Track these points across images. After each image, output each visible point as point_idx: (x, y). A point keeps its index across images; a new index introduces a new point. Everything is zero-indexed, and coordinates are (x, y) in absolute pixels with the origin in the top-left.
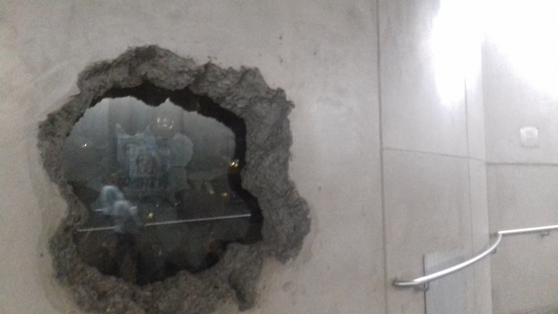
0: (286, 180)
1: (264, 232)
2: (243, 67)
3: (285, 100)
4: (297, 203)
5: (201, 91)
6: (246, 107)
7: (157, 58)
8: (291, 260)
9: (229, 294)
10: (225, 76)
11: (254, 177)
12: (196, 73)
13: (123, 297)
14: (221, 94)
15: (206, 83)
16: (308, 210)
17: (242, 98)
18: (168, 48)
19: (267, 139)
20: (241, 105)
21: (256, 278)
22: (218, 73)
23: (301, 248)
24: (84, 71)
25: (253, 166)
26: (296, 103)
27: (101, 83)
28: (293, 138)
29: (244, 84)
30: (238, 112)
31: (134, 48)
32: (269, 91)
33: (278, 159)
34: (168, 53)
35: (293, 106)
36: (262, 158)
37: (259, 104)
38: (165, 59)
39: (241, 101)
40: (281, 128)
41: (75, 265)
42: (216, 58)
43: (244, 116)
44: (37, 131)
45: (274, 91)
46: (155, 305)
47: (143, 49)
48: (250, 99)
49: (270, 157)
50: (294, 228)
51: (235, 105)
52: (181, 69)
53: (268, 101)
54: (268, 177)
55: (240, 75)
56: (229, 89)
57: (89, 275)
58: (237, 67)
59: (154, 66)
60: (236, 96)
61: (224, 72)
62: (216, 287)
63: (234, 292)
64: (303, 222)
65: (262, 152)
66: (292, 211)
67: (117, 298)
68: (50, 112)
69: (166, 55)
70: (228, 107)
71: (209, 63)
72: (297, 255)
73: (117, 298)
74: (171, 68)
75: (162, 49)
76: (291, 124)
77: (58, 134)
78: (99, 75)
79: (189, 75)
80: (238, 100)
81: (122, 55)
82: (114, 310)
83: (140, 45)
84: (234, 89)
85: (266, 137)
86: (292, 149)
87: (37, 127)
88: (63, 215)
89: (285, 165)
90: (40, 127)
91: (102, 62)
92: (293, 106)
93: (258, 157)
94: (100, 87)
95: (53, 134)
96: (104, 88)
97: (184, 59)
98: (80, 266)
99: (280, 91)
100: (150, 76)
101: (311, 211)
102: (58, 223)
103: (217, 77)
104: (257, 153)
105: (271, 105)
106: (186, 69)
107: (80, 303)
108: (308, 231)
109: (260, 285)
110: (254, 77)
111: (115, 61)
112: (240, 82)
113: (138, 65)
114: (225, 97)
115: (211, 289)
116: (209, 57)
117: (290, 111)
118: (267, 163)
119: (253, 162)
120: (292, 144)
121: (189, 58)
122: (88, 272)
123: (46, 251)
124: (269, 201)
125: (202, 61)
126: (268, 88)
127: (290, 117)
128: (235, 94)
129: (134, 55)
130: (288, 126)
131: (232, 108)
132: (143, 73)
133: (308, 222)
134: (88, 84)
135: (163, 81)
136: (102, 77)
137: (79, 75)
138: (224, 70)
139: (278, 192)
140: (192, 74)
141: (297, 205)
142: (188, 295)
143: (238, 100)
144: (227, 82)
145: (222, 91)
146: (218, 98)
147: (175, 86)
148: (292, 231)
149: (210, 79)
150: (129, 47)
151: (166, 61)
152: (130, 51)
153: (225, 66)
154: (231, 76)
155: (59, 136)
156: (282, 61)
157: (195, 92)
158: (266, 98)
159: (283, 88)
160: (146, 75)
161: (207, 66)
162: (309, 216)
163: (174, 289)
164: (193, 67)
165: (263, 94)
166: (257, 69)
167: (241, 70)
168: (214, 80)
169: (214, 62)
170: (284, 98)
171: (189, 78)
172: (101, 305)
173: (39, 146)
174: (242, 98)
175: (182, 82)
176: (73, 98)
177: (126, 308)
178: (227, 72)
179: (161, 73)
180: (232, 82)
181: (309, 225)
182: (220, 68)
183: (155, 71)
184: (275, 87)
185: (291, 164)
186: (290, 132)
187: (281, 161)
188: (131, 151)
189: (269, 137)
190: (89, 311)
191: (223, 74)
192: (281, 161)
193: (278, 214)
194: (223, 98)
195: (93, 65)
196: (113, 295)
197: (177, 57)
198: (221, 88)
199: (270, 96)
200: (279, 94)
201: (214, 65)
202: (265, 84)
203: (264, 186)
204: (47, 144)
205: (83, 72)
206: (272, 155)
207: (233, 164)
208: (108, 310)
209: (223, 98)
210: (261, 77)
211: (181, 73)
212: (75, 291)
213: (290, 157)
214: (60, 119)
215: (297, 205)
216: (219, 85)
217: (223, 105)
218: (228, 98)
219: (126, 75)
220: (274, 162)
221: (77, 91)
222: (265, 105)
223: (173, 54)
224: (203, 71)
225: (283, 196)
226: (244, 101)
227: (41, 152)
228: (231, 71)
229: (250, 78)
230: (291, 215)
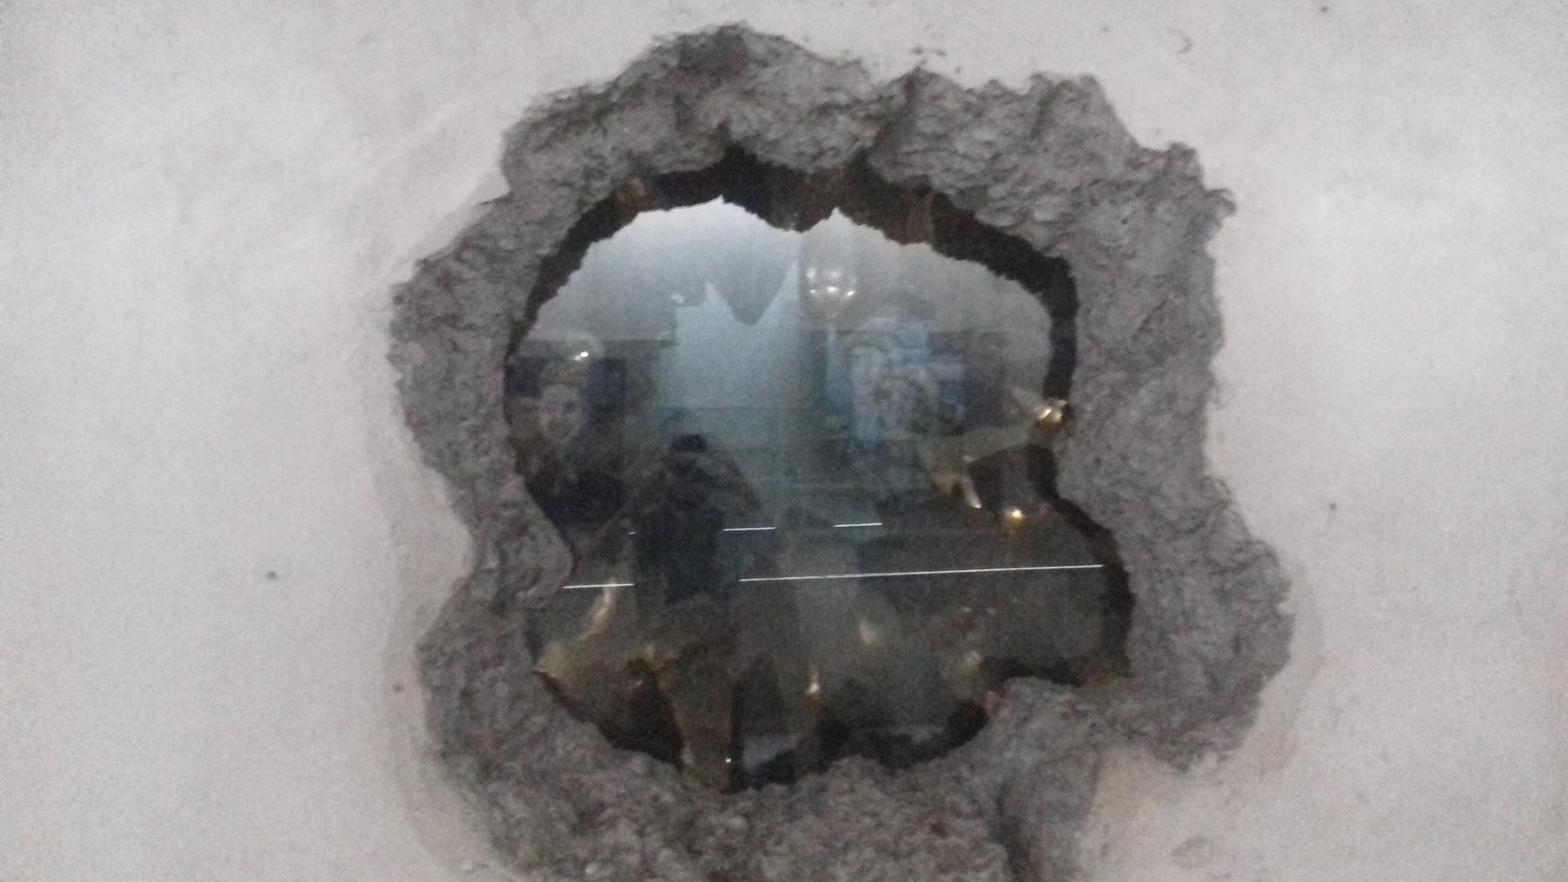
0: (1199, 479)
1: (1136, 651)
2: (1038, 77)
3: (1201, 187)
4: (1241, 558)
5: (908, 172)
6: (1066, 220)
7: (753, 67)
8: (1210, 760)
9: (979, 861)
10: (979, 115)
11: (1089, 460)
12: (873, 108)
13: (641, 833)
14: (969, 177)
15: (919, 144)
16: (1285, 586)
17: (1048, 188)
18: (778, 31)
19: (1144, 328)
20: (1045, 211)
21: (1076, 814)
22: (950, 104)
23: (1250, 722)
24: (522, 123)
25: (1091, 424)
26: (1239, 197)
27: (586, 161)
29: (1051, 138)
30: (1038, 237)
31: (672, 38)
32: (1137, 157)
33: (1171, 398)
34: (779, 48)
35: (1231, 207)
36: (1115, 395)
37: (1105, 205)
38: (776, 69)
39: (1045, 199)
40: (1184, 290)
42: (941, 53)
43: (1062, 249)
44: (389, 315)
45: (1156, 154)
47: (703, 40)
48: (1077, 190)
49: (1143, 392)
50: (1237, 643)
51: (1025, 215)
52: (823, 99)
53: (1138, 195)
55: (1032, 107)
56: (996, 157)
58: (1017, 80)
59: (748, 94)
60: (1024, 181)
61: (973, 99)
62: (939, 830)
63: (999, 851)
64: (1264, 628)
66: (1228, 586)
67: (625, 834)
68: (426, 253)
69: (777, 55)
70: (1003, 221)
71: (918, 70)
72: (1235, 744)
73: (625, 834)
74: (795, 99)
75: (760, 37)
76: (1221, 272)
77: (468, 320)
78: (578, 134)
79: (853, 117)
80: (1033, 196)
81: (636, 64)
82: (609, 871)
83: (690, 27)
84: (1014, 159)
85: (1138, 323)
86: (1222, 365)
87: (390, 300)
88: (459, 567)
89: (1193, 422)
90: (398, 299)
91: (574, 89)
92: (1231, 207)
93: (1106, 391)
94: (589, 174)
95: (453, 320)
96: (602, 174)
97: (830, 64)
99: (1181, 154)
100: (737, 131)
101: (1294, 593)
103: (947, 118)
104: (1102, 378)
105: (1151, 209)
106: (842, 98)
108: (1277, 662)
109: (1089, 841)
110: (1084, 108)
111: (614, 85)
112: (1037, 131)
113: (699, 97)
114: (986, 188)
115: (921, 837)
116: (918, 51)
117: (1219, 225)
118: (1134, 414)
119: (1089, 407)
120: (1221, 346)
121: (850, 58)
122: (559, 742)
123: (409, 675)
124: (1147, 544)
125: (890, 67)
126: (1134, 146)
127: (1217, 246)
128: (1018, 176)
129: (673, 62)
130: (1209, 281)
131: (1013, 227)
132: (715, 122)
133: (1282, 629)
134: (540, 164)
135: (775, 143)
136: (590, 139)
137: (507, 135)
138: (970, 91)
139: (1172, 516)
140: (862, 114)
141: (1244, 566)
142: (846, 847)
143: (1033, 196)
144: (984, 134)
145: (970, 168)
146: (961, 192)
147: (815, 158)
148: (1229, 655)
149: (926, 125)
150: (656, 38)
151: (777, 74)
152: (660, 50)
153: (973, 77)
154: (997, 112)
155: (470, 327)
156: (1188, 46)
157: (890, 176)
158: (1130, 184)
159: (1191, 142)
160: (723, 128)
161: (913, 83)
162: (1284, 608)
164: (863, 90)
165: (1116, 168)
166: (1091, 81)
167: (1033, 88)
168: (940, 129)
169: (934, 65)
170: (1195, 179)
171: (854, 127)
172: (581, 847)
173: (394, 358)
174: (1048, 188)
175: (833, 142)
176: (490, 208)
177: (647, 866)
178: (983, 97)
179: (768, 115)
180: (1008, 134)
182: (956, 88)
183: (748, 109)
184: (1160, 144)
185: (1216, 419)
186: (1213, 302)
188: (858, 371)
189: (1146, 322)
190: (528, 868)
191: (967, 107)
192: (1182, 405)
193: (1178, 591)
194: (979, 192)
195: (547, 103)
196: (612, 823)
197: (811, 57)
198: (965, 156)
199: (1143, 176)
200: (1179, 164)
201: (933, 76)
202: (1123, 132)
203: (1126, 494)
204: (416, 350)
205: (517, 126)
207: (1048, 412)
208: (590, 870)
209: (979, 192)
210: (1107, 109)
211: (825, 111)
212: (494, 803)
213: (1213, 392)
214: (469, 274)
215: (1244, 566)
216: (960, 146)
217: (982, 217)
218: (997, 191)
219: (664, 132)
221: (502, 189)
222: (1127, 211)
223: (797, 47)
224: (900, 99)
225: (1192, 531)
226: (1056, 199)
227: (399, 376)
228: (996, 94)
229: (1067, 116)
230: (1223, 595)
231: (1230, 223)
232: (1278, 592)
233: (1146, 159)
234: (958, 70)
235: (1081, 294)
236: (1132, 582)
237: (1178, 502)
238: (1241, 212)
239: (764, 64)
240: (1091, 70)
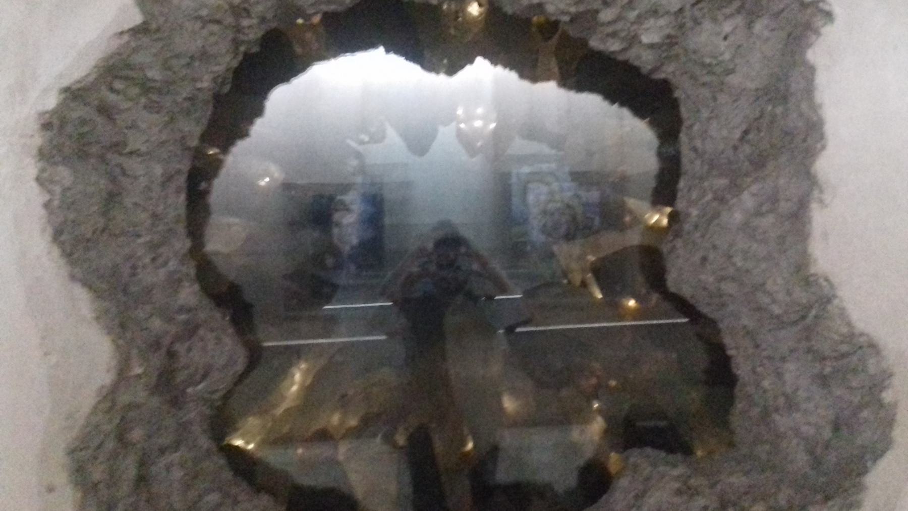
4: (844, 348)
6: (670, 42)
25: (696, 227)
28: (829, 128)
30: (645, 59)
33: (774, 199)
36: (721, 199)
37: (707, 25)
39: (652, 21)
43: (668, 71)
49: (746, 196)
51: (633, 40)
54: (738, 261)
65: (723, 182)
70: (614, 46)
76: (821, 79)
80: (640, 19)
85: (737, 134)
93: (709, 196)
105: (749, 26)
119: (694, 212)
130: (809, 90)
139: (777, 310)
143: (640, 19)
181: (890, 422)
187: (784, 206)
189: (746, 132)
192: (784, 206)
206: (754, 188)
213: (816, 193)
215: (843, 356)
217: (595, 43)
220: (758, 214)
222: (727, 27)
225: (795, 323)
226: (662, 22)
230: (823, 380)
237: (781, 296)
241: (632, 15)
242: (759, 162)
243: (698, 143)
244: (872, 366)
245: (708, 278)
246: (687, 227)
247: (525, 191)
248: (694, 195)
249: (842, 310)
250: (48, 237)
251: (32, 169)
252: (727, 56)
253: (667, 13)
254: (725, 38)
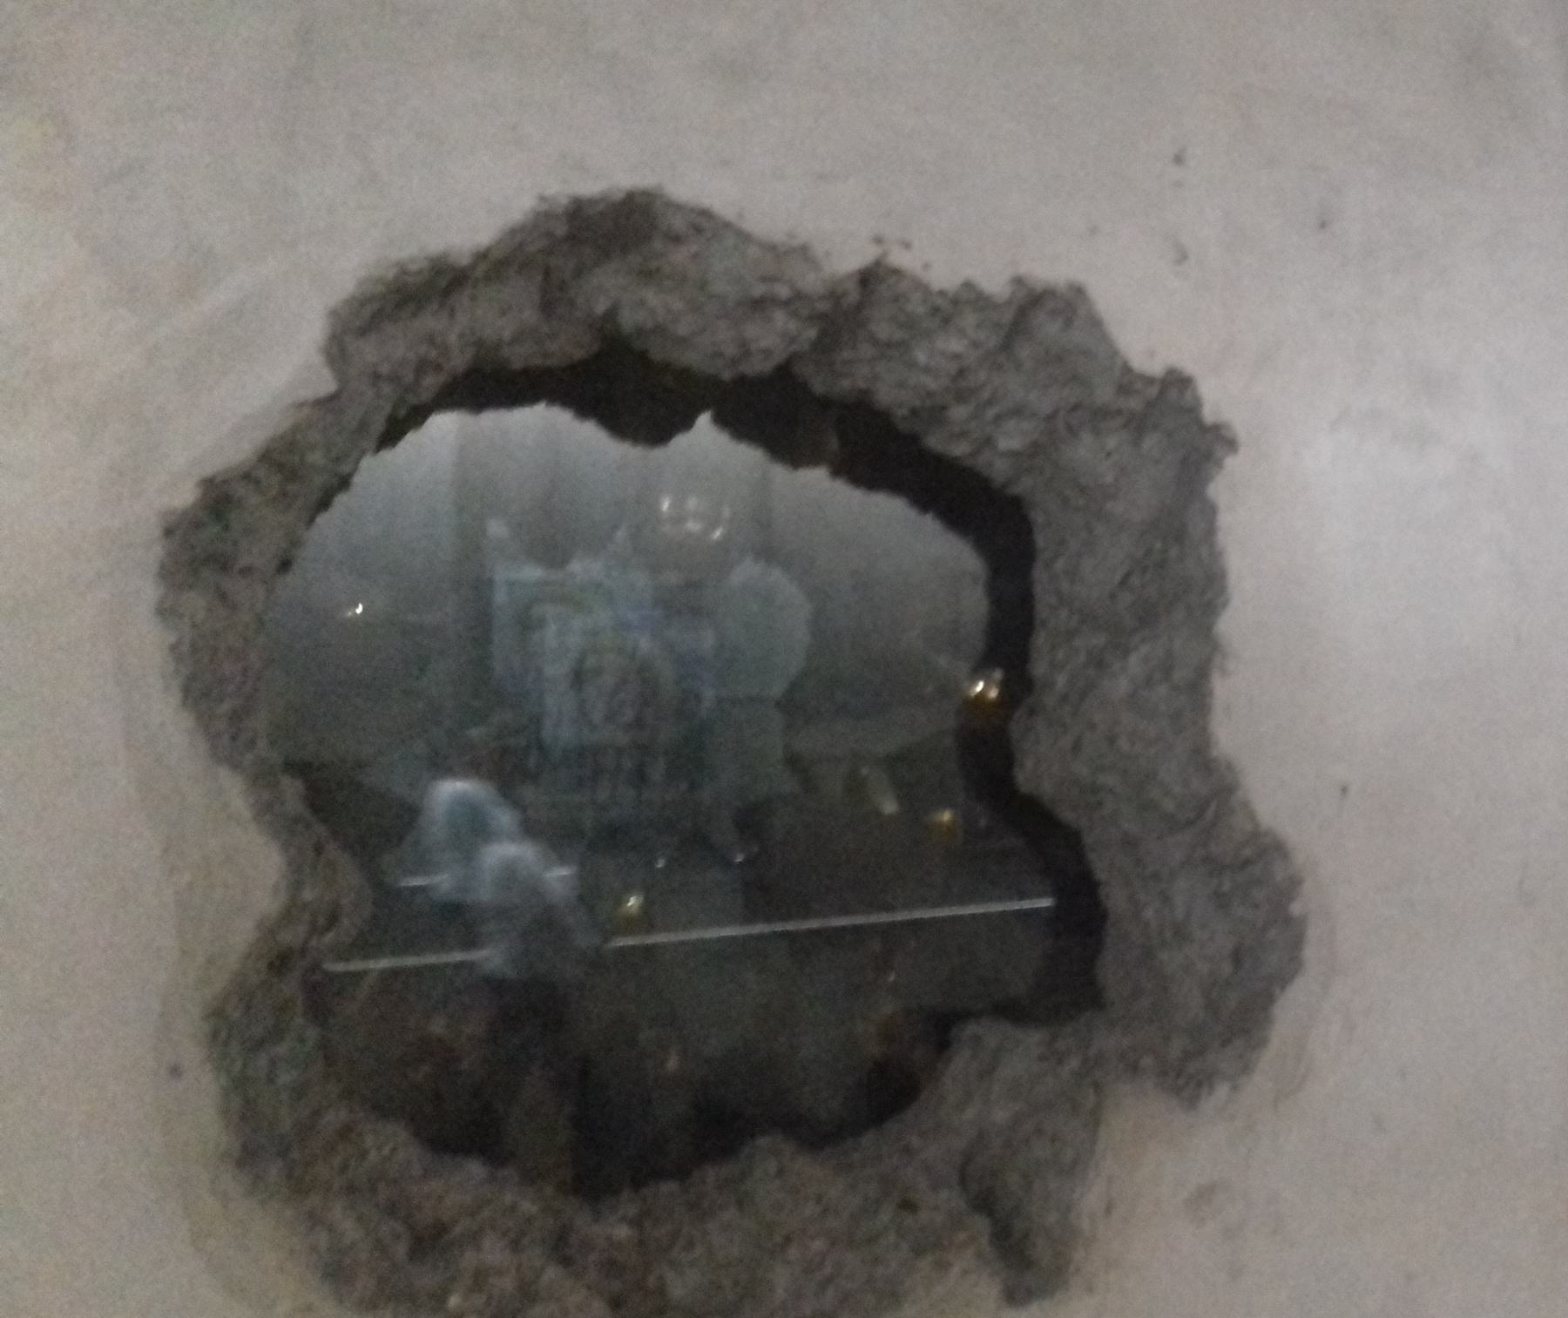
0: (1202, 758)
1: (1111, 972)
2: (1018, 281)
3: (1198, 422)
4: (1247, 852)
5: (846, 384)
6: (1035, 449)
7: (658, 245)
8: (1222, 1090)
9: (962, 1236)
10: (946, 321)
11: (1066, 742)
12: (823, 306)
13: (515, 1246)
14: (930, 394)
15: (866, 350)
16: (1295, 883)
17: (1018, 412)
18: (706, 202)
19: (1124, 582)
20: (1011, 439)
21: (1074, 1169)
22: (916, 307)
23: (1262, 1043)
24: (354, 298)
25: (1064, 698)
26: (1241, 432)
27: (423, 349)
28: (1233, 579)
29: (1025, 352)
30: (998, 469)
31: (564, 201)
32: (1128, 381)
33: (1167, 669)
34: (704, 224)
35: (1231, 445)
36: (1098, 662)
37: (1087, 438)
38: (694, 248)
39: (1011, 424)
40: (1179, 536)
41: (317, 1113)
42: (907, 245)
43: (1023, 486)
44: (157, 551)
45: (1150, 381)
46: (651, 1280)
47: (601, 207)
48: (1051, 417)
49: (1133, 659)
50: (1237, 957)
51: (988, 442)
52: (759, 290)
53: (1125, 426)
54: (1123, 744)
55: (1008, 316)
56: (961, 372)
57: (373, 1156)
58: (995, 283)
59: (648, 275)
60: (990, 402)
61: (939, 302)
62: (908, 1206)
63: (981, 1224)
64: (1272, 933)
65: (1099, 640)
66: (1227, 886)
67: (493, 1252)
68: (208, 470)
69: (698, 230)
70: (959, 449)
71: (878, 263)
72: (1246, 1069)
73: (493, 1252)
74: (719, 287)
75: (679, 207)
76: (1224, 519)
77: (243, 561)
78: (414, 315)
79: (795, 314)
80: (998, 418)
81: (513, 232)
82: (479, 1300)
83: (589, 188)
84: (982, 376)
85: (1118, 577)
86: (1228, 625)
87: (157, 532)
89: (1197, 691)
90: (168, 532)
91: (426, 258)
92: (1231, 445)
93: (1082, 658)
94: (422, 367)
95: (223, 564)
96: (438, 367)
97: (772, 248)
98: (335, 1117)
99: (1177, 382)
100: (629, 319)
101: (1308, 887)
102: (242, 935)
103: (910, 323)
104: (1078, 642)
105: (1136, 443)
106: (783, 291)
107: (336, 1272)
108: (1292, 966)
109: (1090, 1199)
110: (1068, 323)
111: (482, 256)
112: (1007, 346)
113: (579, 273)
114: (944, 408)
115: (886, 1215)
116: (878, 240)
117: (1219, 464)
118: (1122, 686)
119: (1061, 680)
120: (1225, 605)
121: (795, 243)
122: (369, 1140)
123: (192, 1054)
124: (1130, 843)
125: (848, 259)
126: (1127, 369)
127: (1218, 490)
128: (986, 394)
129: (561, 230)
130: (1211, 531)
132: (601, 307)
133: (1293, 933)
134: (368, 352)
135: (683, 341)
136: (430, 321)
137: (334, 314)
138: (942, 293)
139: (1169, 805)
140: (805, 312)
141: (1247, 863)
142: (788, 1239)
143: (998, 418)
144: (955, 345)
145: (931, 384)
146: (914, 412)
147: (734, 362)
148: (1227, 968)
149: (883, 329)
150: (542, 199)
151: (695, 256)
152: (548, 215)
153: (943, 275)
154: (969, 319)
155: (246, 571)
156: (1182, 257)
157: (818, 386)
158: (1119, 412)
159: (1189, 367)
160: (611, 314)
161: (869, 278)
162: (1296, 908)
163: (729, 1214)
164: (811, 282)
165: (1104, 394)
166: (1079, 291)
167: (1013, 293)
168: (898, 335)
169: (899, 258)
170: (1192, 411)
171: (792, 326)
172: (426, 1278)
173: (165, 612)
174: (1018, 412)
175: (764, 344)
176: (306, 411)
177: (528, 1292)
178: (955, 302)
179: (677, 305)
180: (975, 345)
181: (1297, 943)
182: (921, 286)
183: (652, 297)
184: (1155, 368)
185: (1221, 688)
186: (1216, 555)
187: (1181, 675)
189: (1127, 576)
190: (373, 1306)
191: (936, 310)
192: (1181, 675)
193: (1166, 899)
194: (935, 413)
195: (391, 274)
196: (474, 1238)
197: (745, 238)
198: (927, 370)
199: (1134, 404)
200: (1173, 394)
201: (897, 272)
202: (1114, 353)
203: (1109, 780)
204: (196, 603)
205: (348, 302)
206: (1144, 649)
207: (980, 687)
208: (454, 1301)
209: (935, 413)
210: (1096, 323)
211: (759, 305)
212: (314, 1220)
214: (254, 500)
215: (1247, 863)
216: (921, 357)
217: (935, 442)
218: (959, 413)
219: (530, 316)
220: (1149, 682)
221: (326, 384)
222: (1111, 443)
223: (727, 225)
224: (854, 296)
225: (1190, 823)
226: (1026, 425)
227: (172, 639)
228: (970, 298)
229: (1048, 328)
230: (1221, 901)
231: (1233, 464)
232: (1293, 885)
233: (1139, 386)
234: (926, 266)
235: (1040, 540)
236: (1103, 892)
237: (1177, 789)
238: (1243, 450)
239: (677, 239)
240: (1081, 277)
241: (991, 413)
242: (1147, 617)
243: (1065, 586)
244: (1279, 874)
245: (1081, 770)
246: (1050, 700)
247: (526, 623)
248: (1060, 655)
249: (1246, 805)
250: (175, 698)
251: (149, 592)
252: (1109, 479)
253: (1034, 415)
254: (1109, 454)
